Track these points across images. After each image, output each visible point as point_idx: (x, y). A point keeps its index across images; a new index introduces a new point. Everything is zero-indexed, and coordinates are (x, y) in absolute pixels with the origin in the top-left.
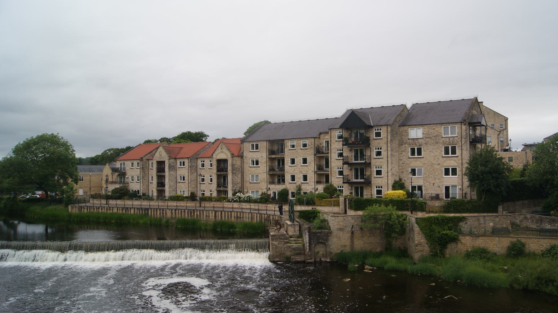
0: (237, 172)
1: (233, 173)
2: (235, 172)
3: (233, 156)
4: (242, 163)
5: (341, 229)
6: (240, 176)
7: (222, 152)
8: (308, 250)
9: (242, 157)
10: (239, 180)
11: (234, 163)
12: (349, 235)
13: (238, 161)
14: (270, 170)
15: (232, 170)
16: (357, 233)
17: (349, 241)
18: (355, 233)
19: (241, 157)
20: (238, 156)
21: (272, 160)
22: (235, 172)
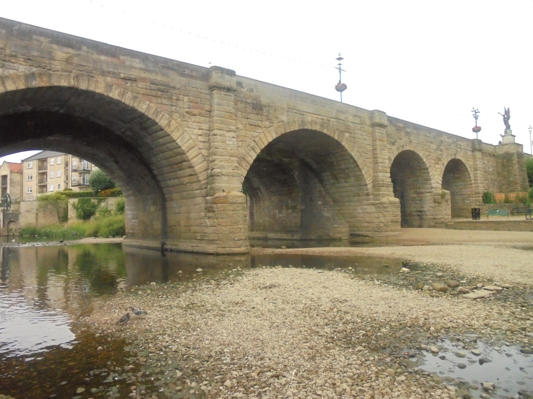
0: (16, 185)
1: (11, 186)
2: (13, 185)
3: (11, 172)
4: (22, 178)
5: (28, 211)
6: (19, 188)
7: (4, 170)
8: (2, 226)
9: (21, 173)
10: (18, 192)
11: (13, 177)
12: (35, 215)
13: (17, 177)
14: (39, 183)
15: (11, 183)
16: (40, 214)
17: (35, 220)
18: (39, 214)
19: (21, 172)
20: (17, 173)
21: (40, 174)
22: (13, 185)
